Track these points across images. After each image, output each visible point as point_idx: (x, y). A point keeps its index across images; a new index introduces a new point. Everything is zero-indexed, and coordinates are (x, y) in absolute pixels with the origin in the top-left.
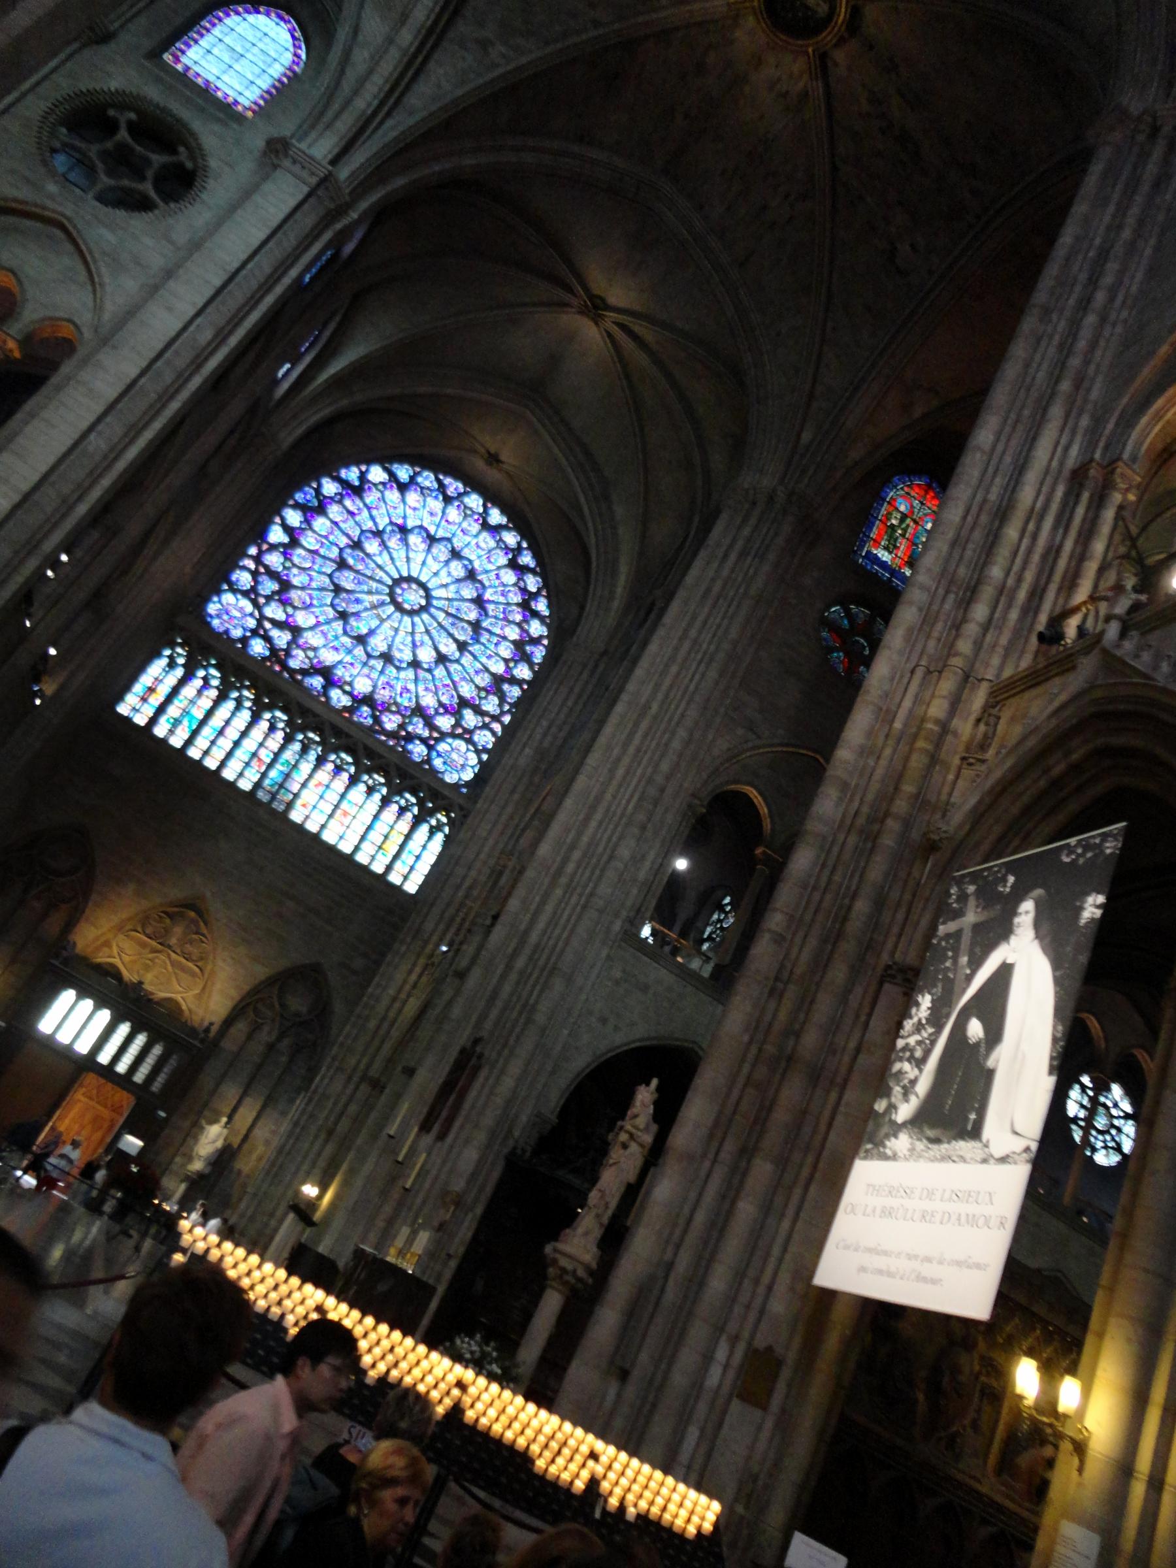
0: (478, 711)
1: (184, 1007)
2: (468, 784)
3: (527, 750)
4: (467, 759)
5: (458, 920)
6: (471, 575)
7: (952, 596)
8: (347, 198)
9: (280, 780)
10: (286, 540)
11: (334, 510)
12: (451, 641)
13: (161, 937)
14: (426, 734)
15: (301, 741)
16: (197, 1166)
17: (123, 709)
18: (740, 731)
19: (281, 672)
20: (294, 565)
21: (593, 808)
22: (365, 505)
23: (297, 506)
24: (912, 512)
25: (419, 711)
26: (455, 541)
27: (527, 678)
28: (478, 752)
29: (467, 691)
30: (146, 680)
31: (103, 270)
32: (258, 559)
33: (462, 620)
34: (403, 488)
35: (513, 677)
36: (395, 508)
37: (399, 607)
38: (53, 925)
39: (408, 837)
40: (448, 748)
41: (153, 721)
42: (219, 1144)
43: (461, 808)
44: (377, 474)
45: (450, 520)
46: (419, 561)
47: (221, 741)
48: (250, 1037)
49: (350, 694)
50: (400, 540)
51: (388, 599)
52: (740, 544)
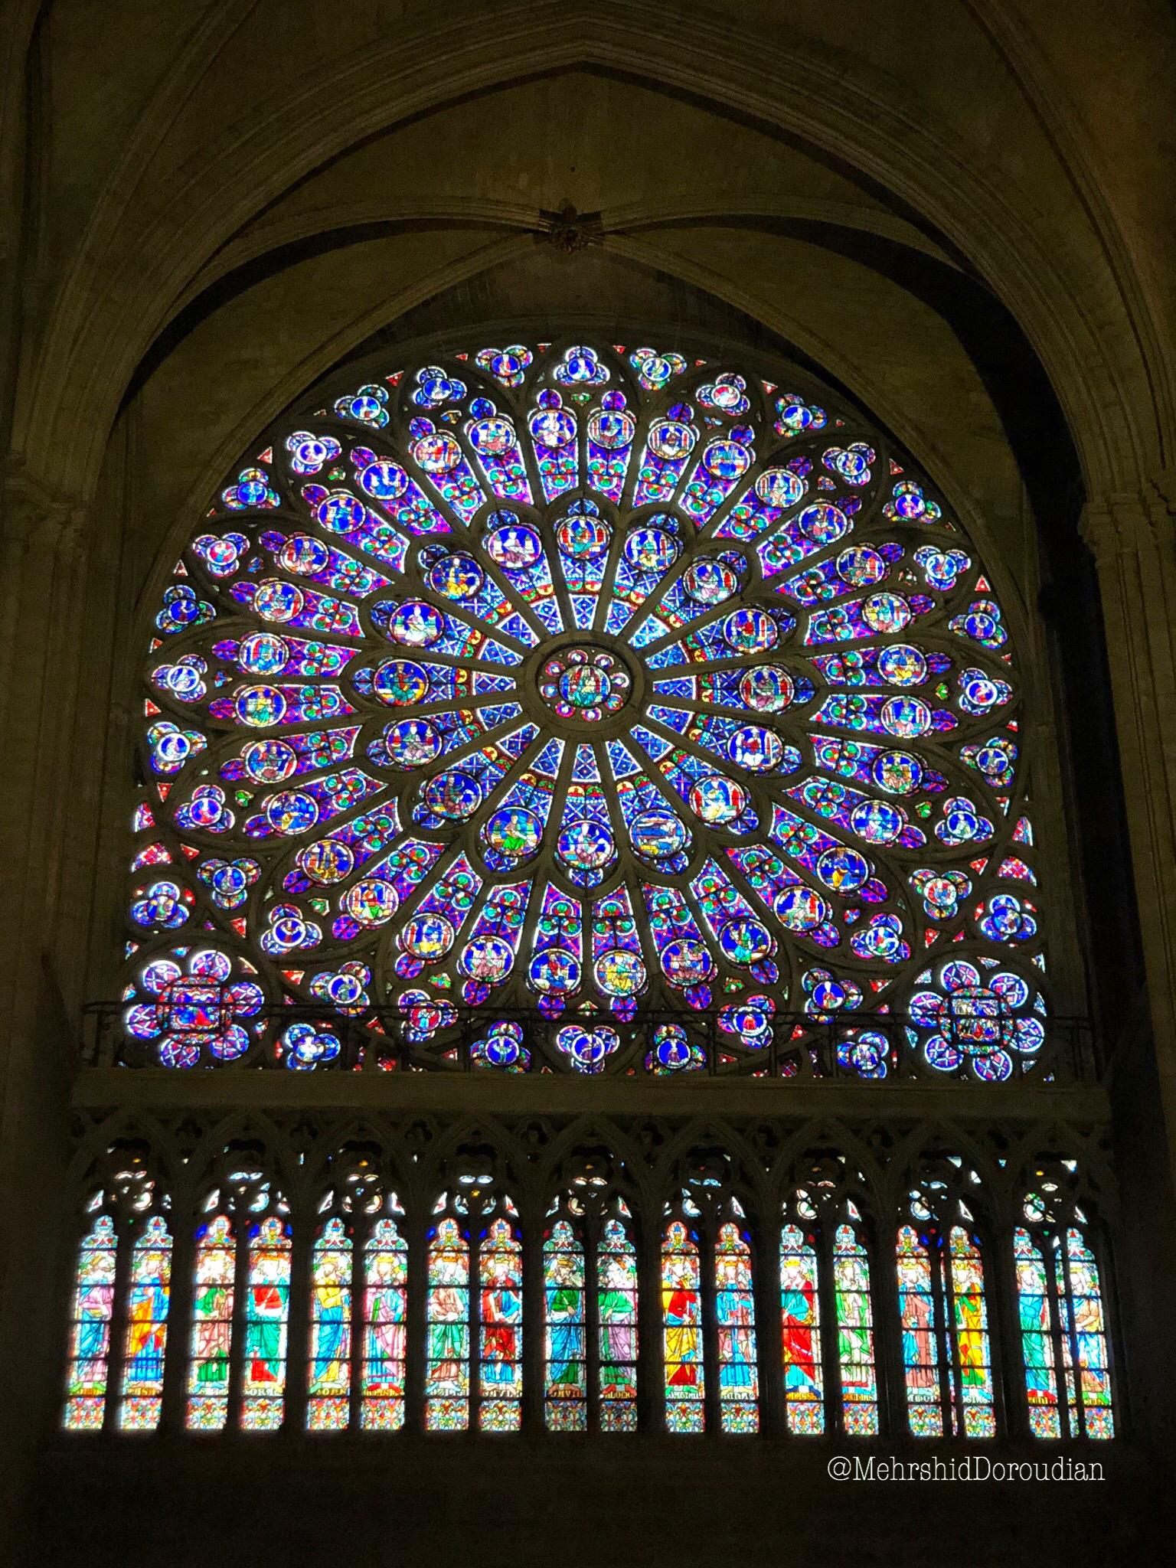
0: (944, 860)
4: (1000, 997)
9: (579, 1350)
10: (201, 741)
11: (269, 601)
12: (755, 730)
15: (564, 1214)
20: (262, 791)
25: (797, 951)
26: (598, 486)
30: (91, 1304)
32: (167, 830)
33: (747, 663)
34: (390, 443)
36: (404, 501)
37: (577, 733)
39: (1000, 1292)
43: (1085, 1131)
44: (309, 450)
45: (551, 441)
47: (373, 1344)
49: (602, 1018)
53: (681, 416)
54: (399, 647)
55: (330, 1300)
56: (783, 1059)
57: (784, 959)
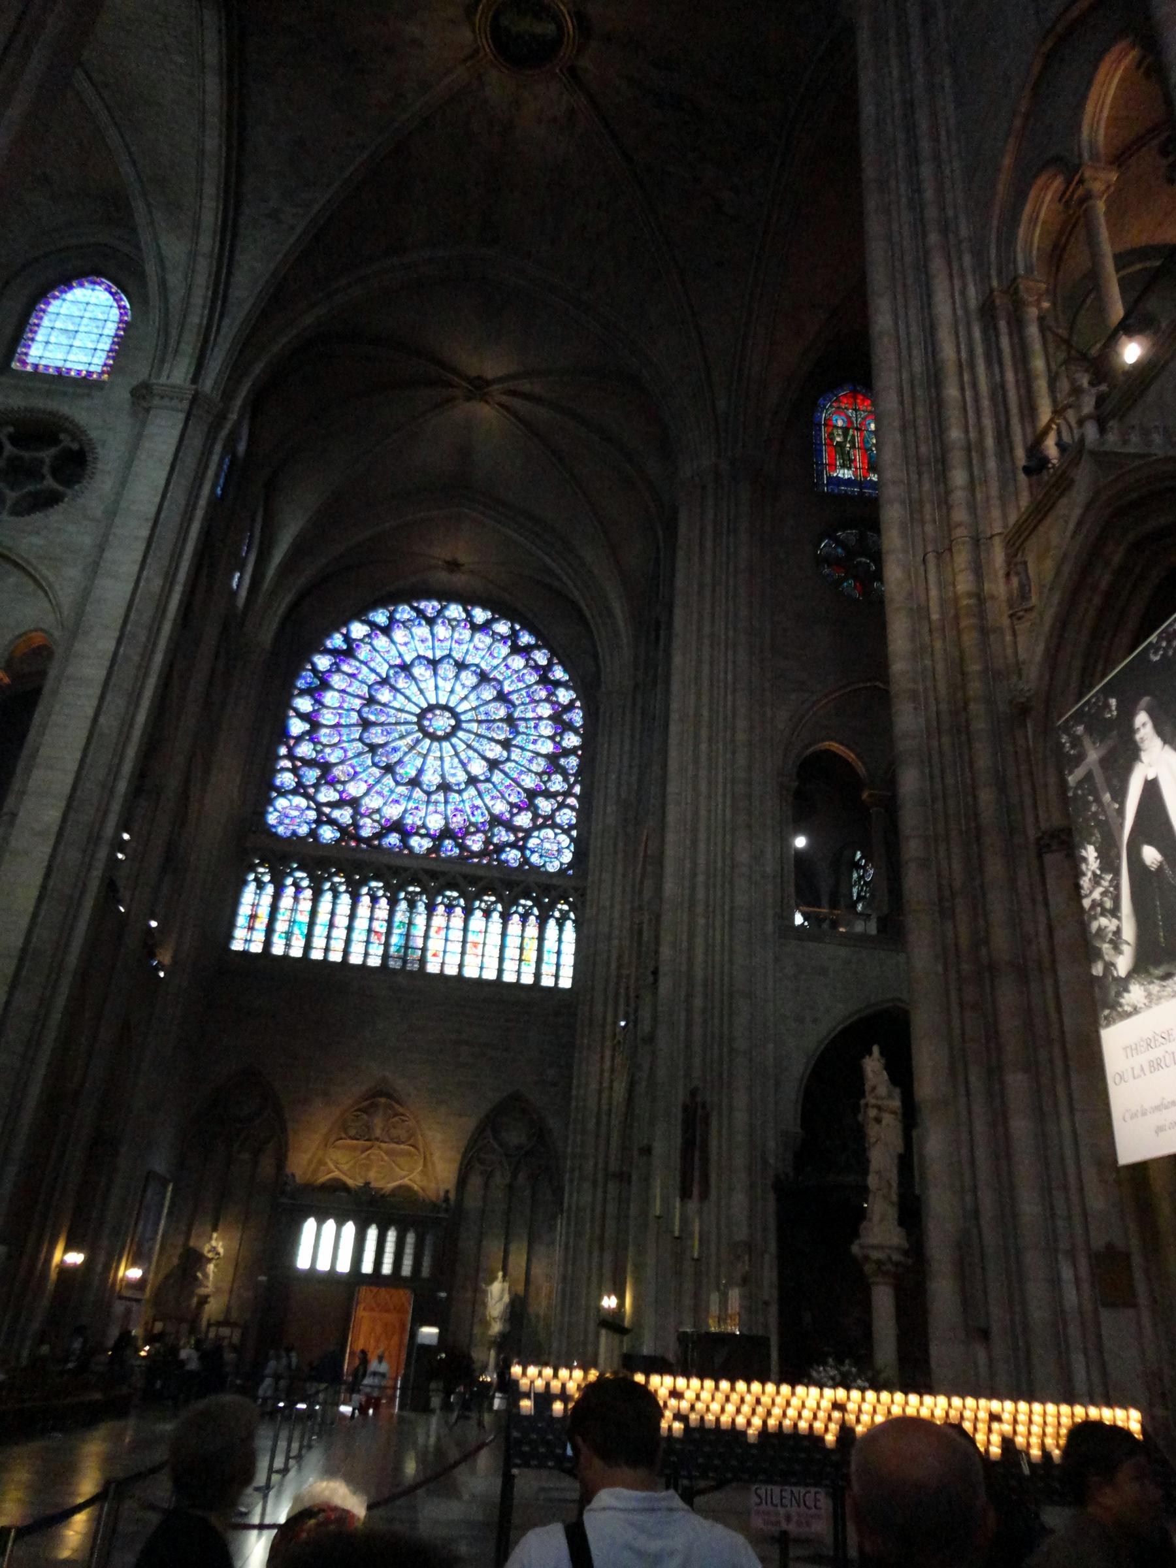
0: (548, 795)
1: (416, 1187)
2: (571, 865)
3: (609, 810)
5: (622, 991)
6: (484, 677)
7: (926, 476)
8: (221, 405)
9: (403, 942)
10: (307, 727)
11: (336, 680)
12: (493, 744)
13: (366, 1134)
14: (512, 838)
15: (405, 898)
16: (496, 1328)
17: (237, 946)
18: (793, 696)
19: (358, 845)
20: (325, 746)
21: (695, 830)
22: (362, 662)
23: (302, 693)
24: (852, 423)
25: (495, 820)
26: (454, 654)
27: (577, 744)
28: (566, 832)
29: (529, 782)
30: (244, 910)
31: (45, 572)
32: (291, 756)
33: (494, 721)
34: (386, 631)
35: (564, 749)
36: (388, 652)
37: (434, 737)
38: (266, 1166)
39: (541, 939)
40: (538, 841)
41: (268, 943)
42: (506, 1299)
43: (576, 890)
44: (358, 630)
46: (432, 688)
47: (335, 933)
48: (486, 1185)
49: (428, 835)
50: (406, 677)
51: (420, 735)
52: (710, 529)
53: (487, 634)
54: (379, 703)
55: (323, 917)
56: (485, 856)
57: (490, 823)
